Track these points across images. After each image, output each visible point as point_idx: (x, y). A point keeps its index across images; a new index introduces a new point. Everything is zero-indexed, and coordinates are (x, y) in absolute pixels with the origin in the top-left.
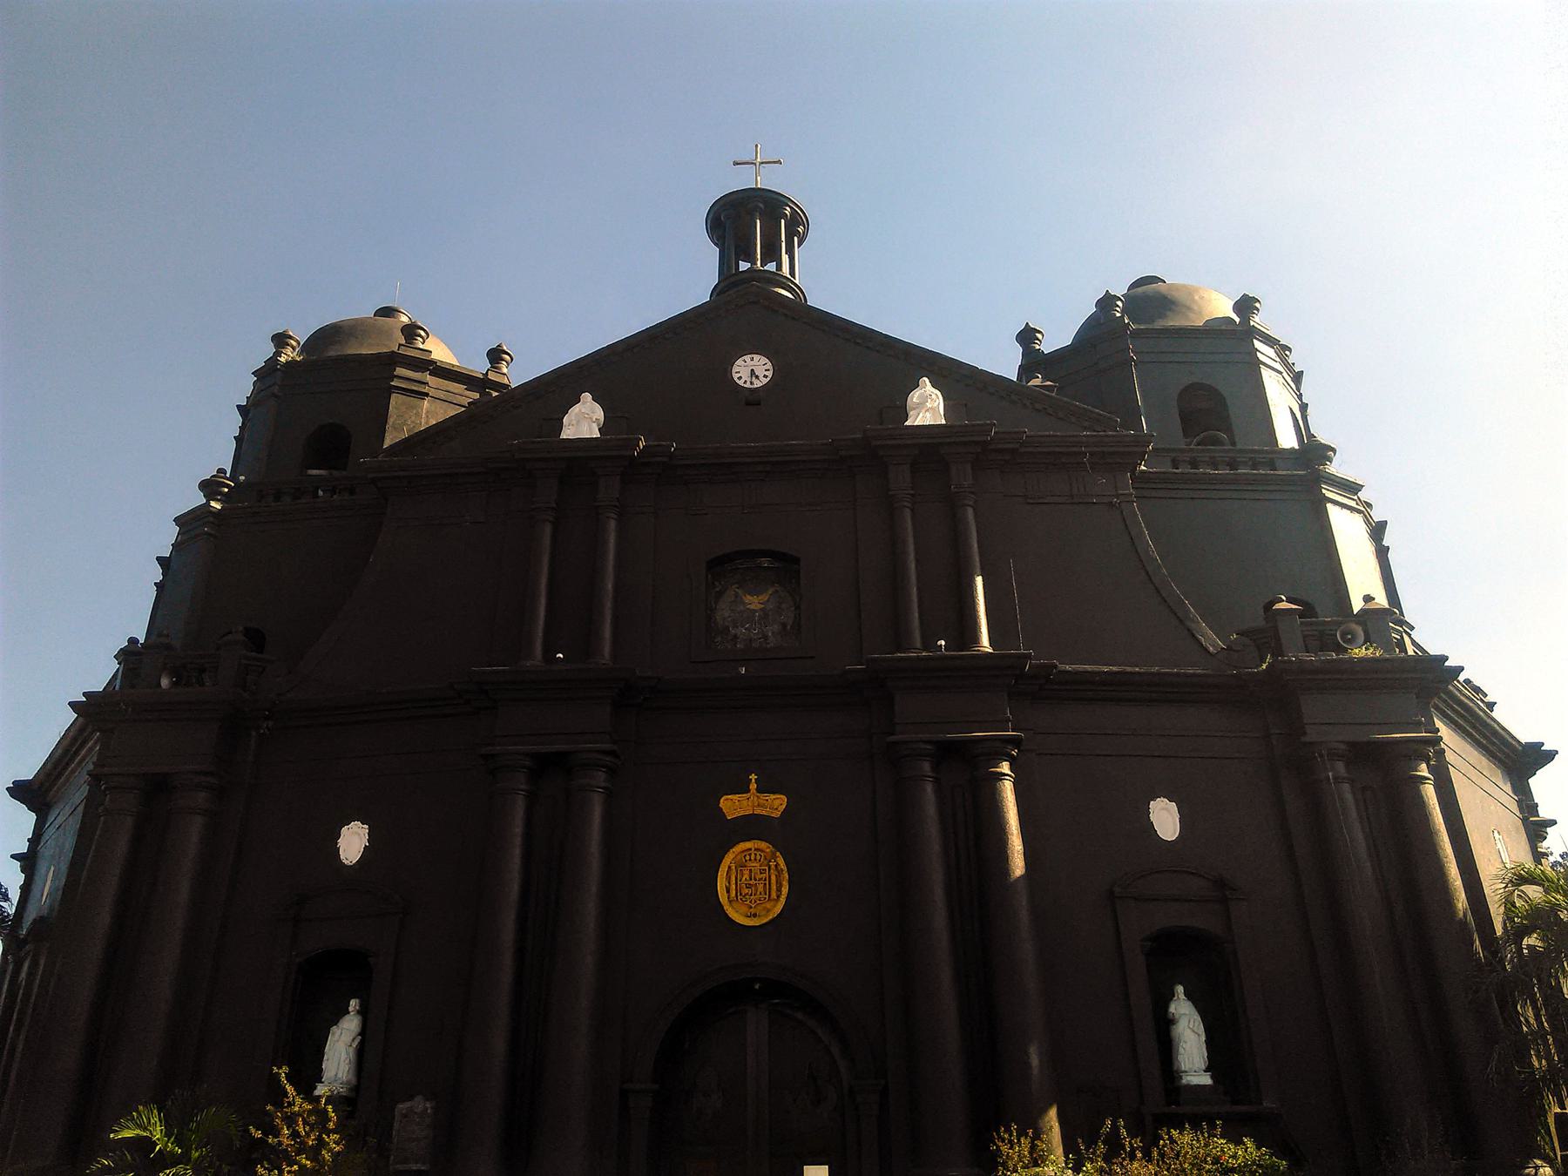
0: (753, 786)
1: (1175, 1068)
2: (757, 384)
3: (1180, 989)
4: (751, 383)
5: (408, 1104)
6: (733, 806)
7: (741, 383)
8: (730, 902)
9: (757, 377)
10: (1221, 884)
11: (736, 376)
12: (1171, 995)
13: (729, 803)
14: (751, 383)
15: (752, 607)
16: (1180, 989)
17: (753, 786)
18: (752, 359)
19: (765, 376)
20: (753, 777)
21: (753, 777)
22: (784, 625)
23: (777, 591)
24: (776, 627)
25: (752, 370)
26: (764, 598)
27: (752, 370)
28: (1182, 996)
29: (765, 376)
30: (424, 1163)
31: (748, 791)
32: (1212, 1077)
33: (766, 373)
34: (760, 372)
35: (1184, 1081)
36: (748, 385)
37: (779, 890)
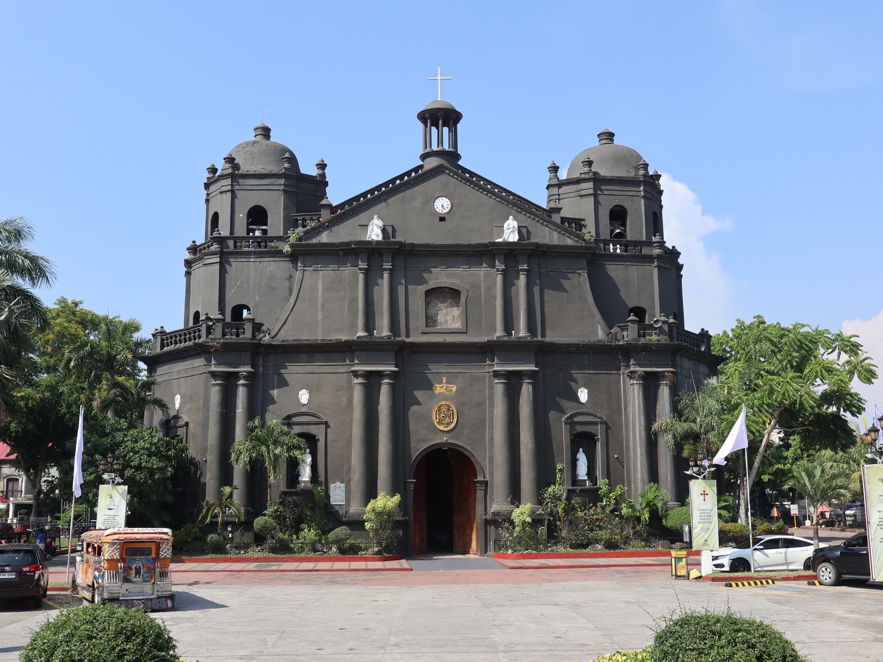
1: (577, 474)
3: (581, 450)
5: (335, 484)
7: (437, 210)
8: (437, 422)
9: (444, 208)
11: (435, 207)
12: (578, 451)
16: (581, 450)
17: (444, 381)
18: (442, 199)
19: (447, 208)
20: (444, 378)
21: (444, 378)
22: (454, 316)
23: (451, 302)
24: (451, 317)
27: (442, 205)
28: (582, 452)
30: (342, 502)
31: (442, 383)
32: (588, 477)
34: (445, 206)
35: (579, 478)
36: (440, 212)
37: (453, 418)
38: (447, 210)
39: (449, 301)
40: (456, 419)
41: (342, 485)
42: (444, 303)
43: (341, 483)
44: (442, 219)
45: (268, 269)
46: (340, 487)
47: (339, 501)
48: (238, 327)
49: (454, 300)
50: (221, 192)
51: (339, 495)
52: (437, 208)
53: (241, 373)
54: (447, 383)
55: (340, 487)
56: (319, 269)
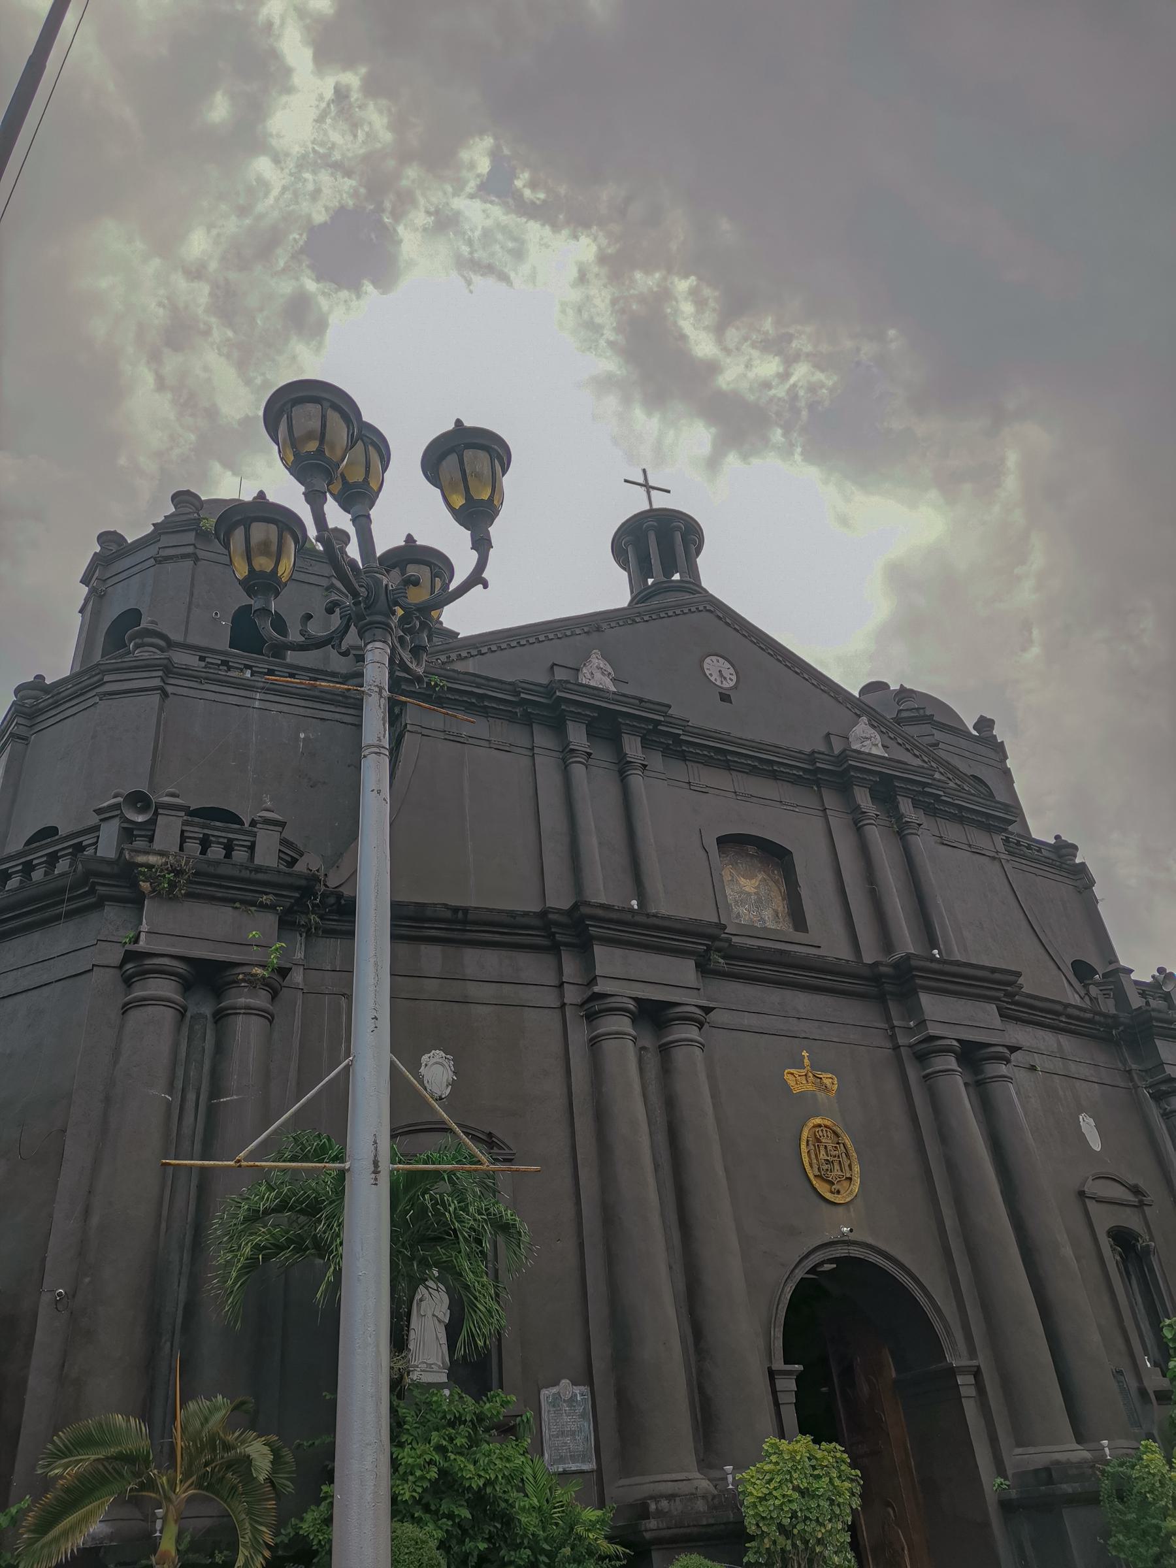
0: (806, 1061)
2: (726, 685)
4: (722, 682)
5: (554, 1390)
6: (797, 1081)
7: (712, 679)
9: (725, 678)
10: (1136, 1190)
13: (790, 1077)
14: (722, 682)
15: (747, 889)
19: (731, 680)
25: (720, 671)
26: (755, 882)
27: (720, 672)
29: (731, 680)
33: (731, 676)
37: (850, 1166)
38: (732, 684)
39: (760, 877)
40: (856, 1168)
41: (577, 1390)
42: (751, 878)
43: (575, 1383)
44: (725, 698)
45: (302, 736)
46: (573, 1399)
47: (574, 1459)
48: (230, 840)
49: (769, 875)
50: (159, 560)
51: (573, 1433)
52: (711, 675)
53: (246, 969)
54: (813, 1067)
55: (573, 1399)
56: (462, 740)
